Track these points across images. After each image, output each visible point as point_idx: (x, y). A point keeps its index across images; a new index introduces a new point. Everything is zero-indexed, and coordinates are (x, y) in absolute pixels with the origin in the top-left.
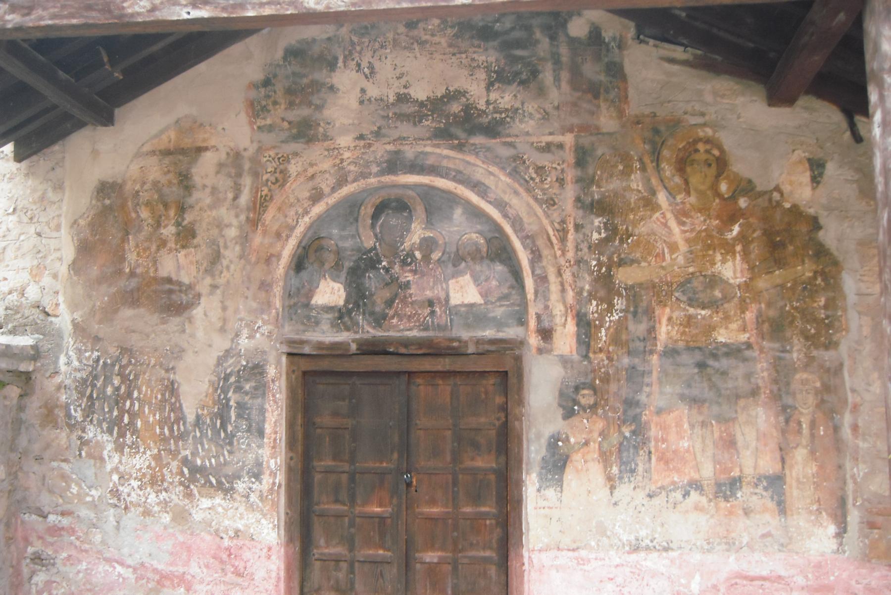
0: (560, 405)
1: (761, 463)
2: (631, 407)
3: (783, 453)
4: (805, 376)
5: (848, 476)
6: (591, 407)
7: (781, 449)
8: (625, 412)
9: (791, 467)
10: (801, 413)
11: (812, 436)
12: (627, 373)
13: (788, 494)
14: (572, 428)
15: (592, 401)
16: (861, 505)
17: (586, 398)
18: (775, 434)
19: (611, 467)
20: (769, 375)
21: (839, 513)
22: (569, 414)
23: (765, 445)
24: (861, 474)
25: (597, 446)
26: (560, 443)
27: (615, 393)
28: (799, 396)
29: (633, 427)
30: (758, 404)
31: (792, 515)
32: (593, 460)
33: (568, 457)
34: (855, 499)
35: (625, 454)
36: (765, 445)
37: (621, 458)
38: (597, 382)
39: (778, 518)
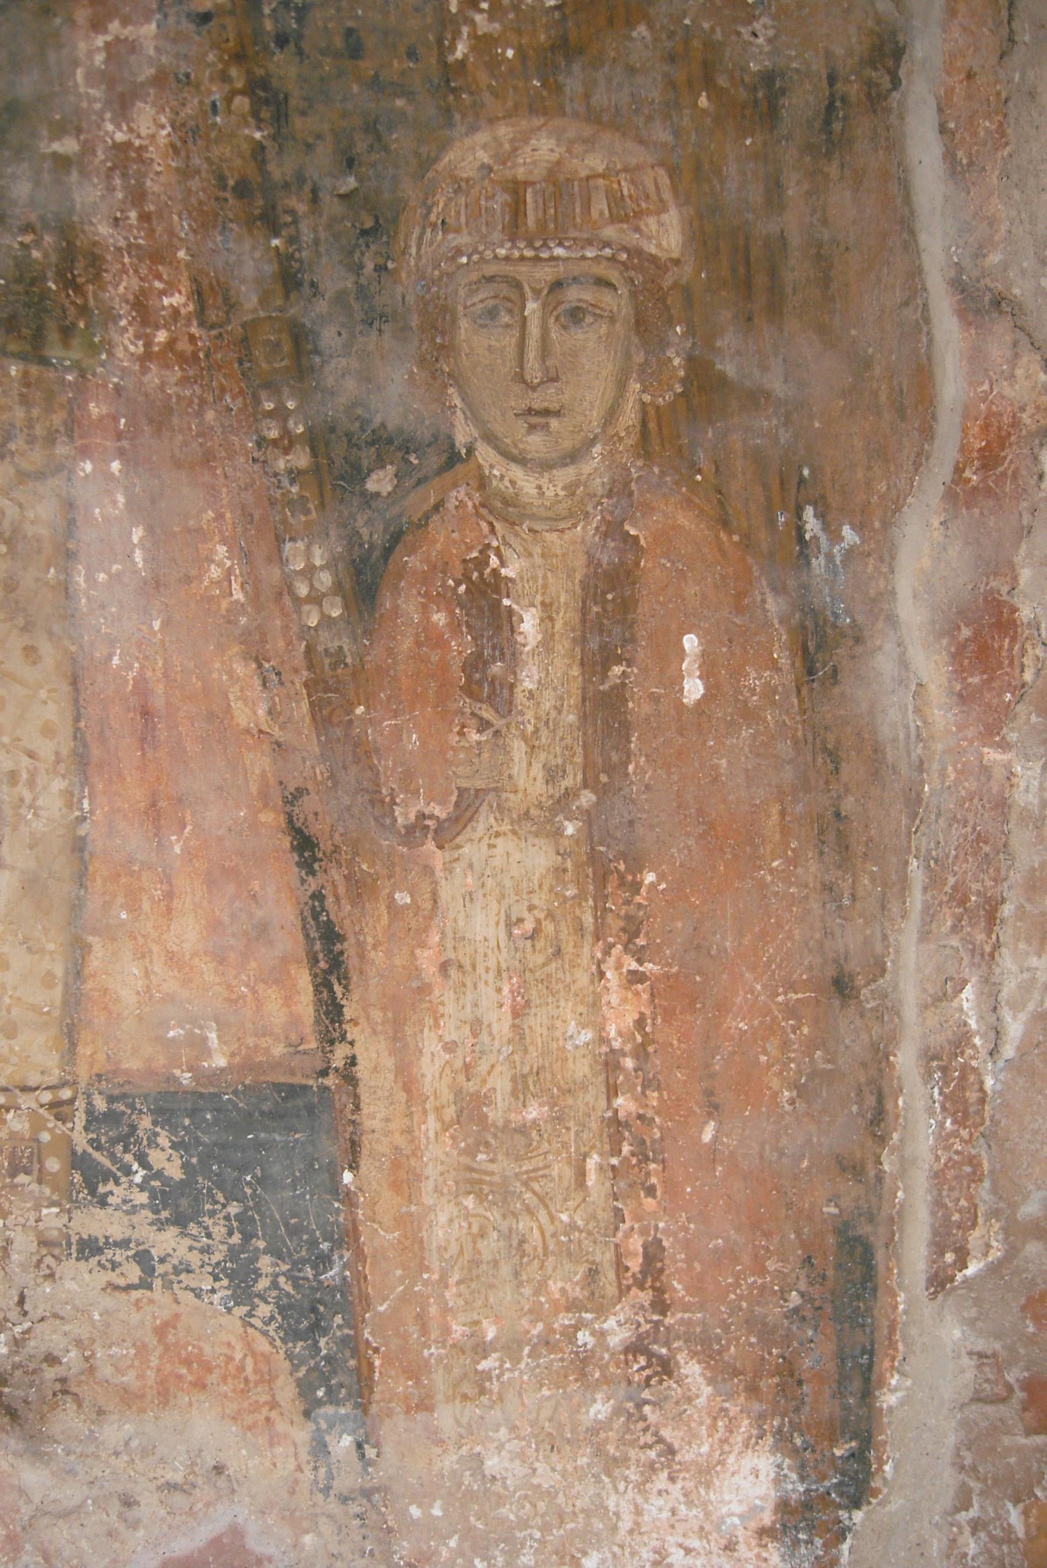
1: (123, 977)
3: (331, 883)
4: (543, 149)
5: (905, 1059)
7: (304, 845)
9: (408, 1004)
10: (505, 509)
11: (606, 714)
13: (379, 1236)
16: (994, 1269)
18: (250, 710)
20: (188, 134)
21: (817, 1356)
23: (156, 814)
24: (1015, 1027)
28: (481, 345)
30: (74, 425)
31: (425, 1405)
34: (949, 1241)
36: (156, 814)
39: (302, 1434)
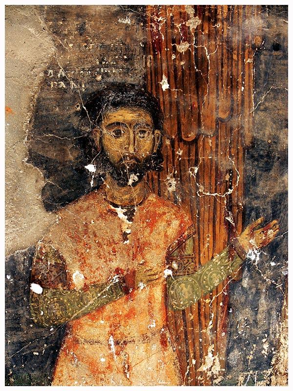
0: (36, 159)
2: (267, 169)
6: (140, 167)
8: (250, 183)
12: (256, 59)
14: (76, 239)
15: (146, 145)
17: (126, 134)
19: (200, 358)
22: (65, 188)
25: (158, 293)
26: (36, 288)
27: (219, 121)
29: (271, 233)
32: (145, 338)
33: (63, 330)
35: (243, 316)
37: (229, 327)
38: (165, 86)
